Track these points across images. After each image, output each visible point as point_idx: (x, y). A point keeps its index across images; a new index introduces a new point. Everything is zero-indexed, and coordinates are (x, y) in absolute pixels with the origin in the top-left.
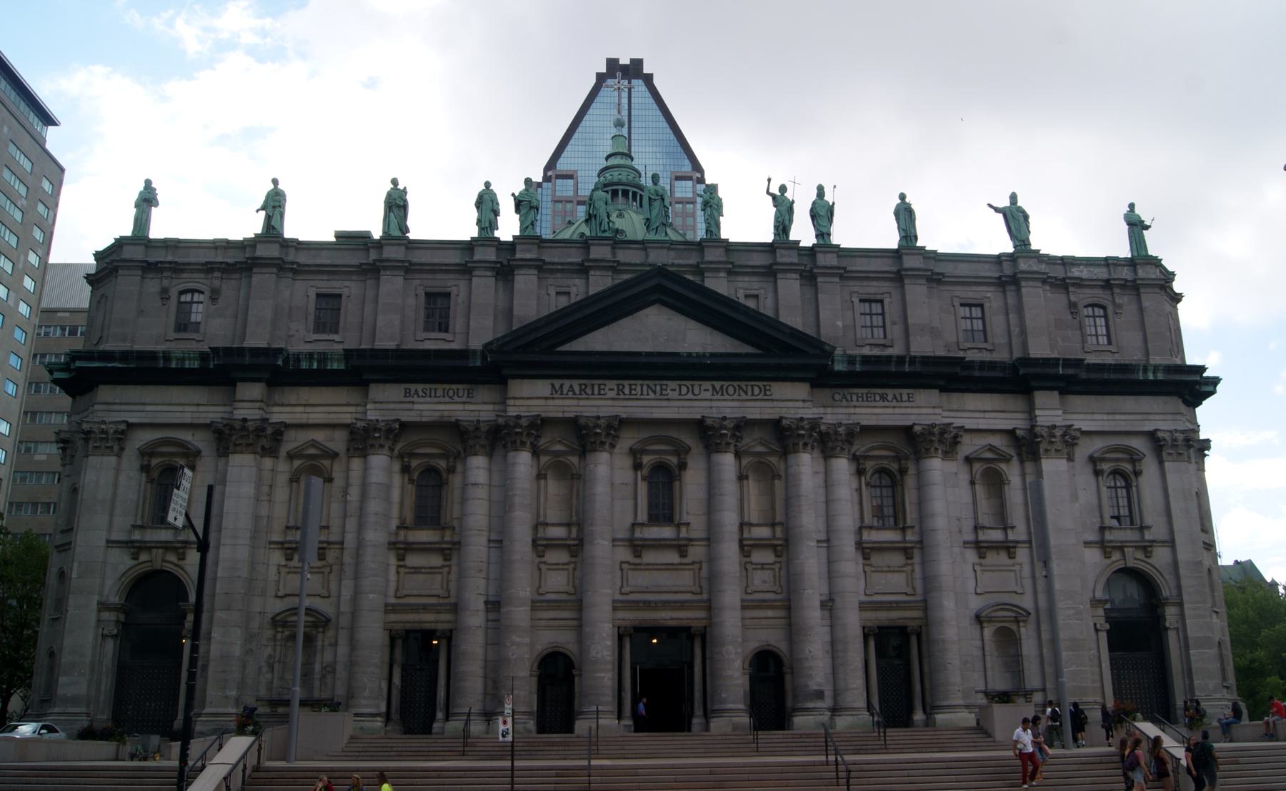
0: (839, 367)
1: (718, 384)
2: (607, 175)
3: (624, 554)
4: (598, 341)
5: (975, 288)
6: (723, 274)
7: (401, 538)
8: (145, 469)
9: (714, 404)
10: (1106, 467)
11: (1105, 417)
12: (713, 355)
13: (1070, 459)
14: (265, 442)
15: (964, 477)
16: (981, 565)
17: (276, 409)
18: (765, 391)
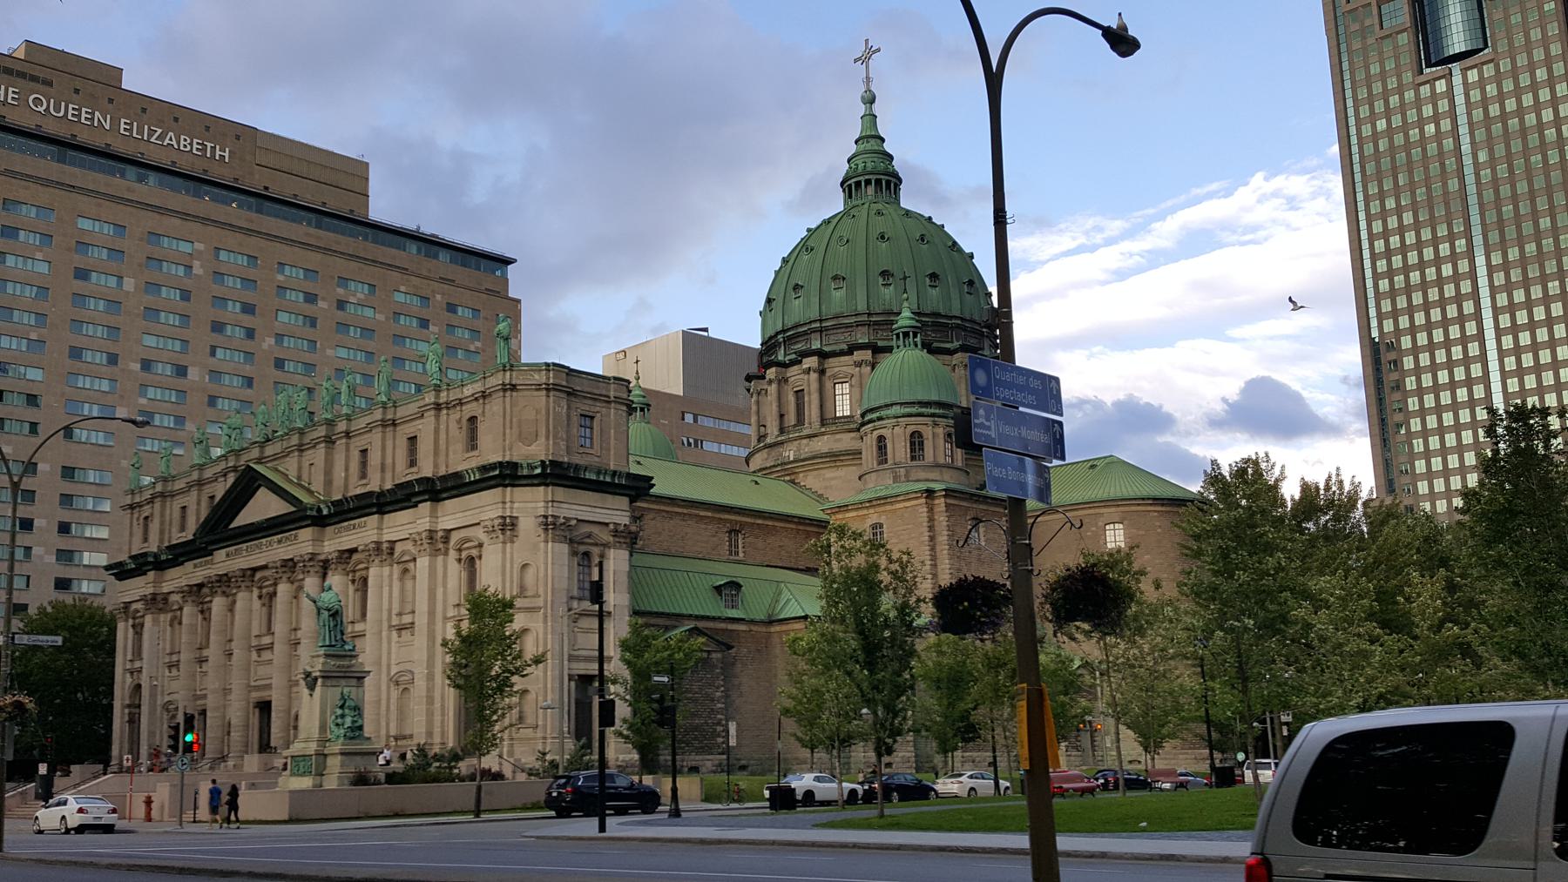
0: (325, 512)
1: (279, 536)
2: (859, 162)
3: (254, 655)
4: (245, 517)
5: (414, 423)
6: (296, 454)
7: (198, 656)
8: (133, 626)
9: (279, 550)
10: (464, 554)
11: (461, 515)
12: (267, 520)
13: (435, 552)
14: (161, 606)
15: (396, 576)
16: (398, 642)
17: (164, 584)
18: (296, 536)
